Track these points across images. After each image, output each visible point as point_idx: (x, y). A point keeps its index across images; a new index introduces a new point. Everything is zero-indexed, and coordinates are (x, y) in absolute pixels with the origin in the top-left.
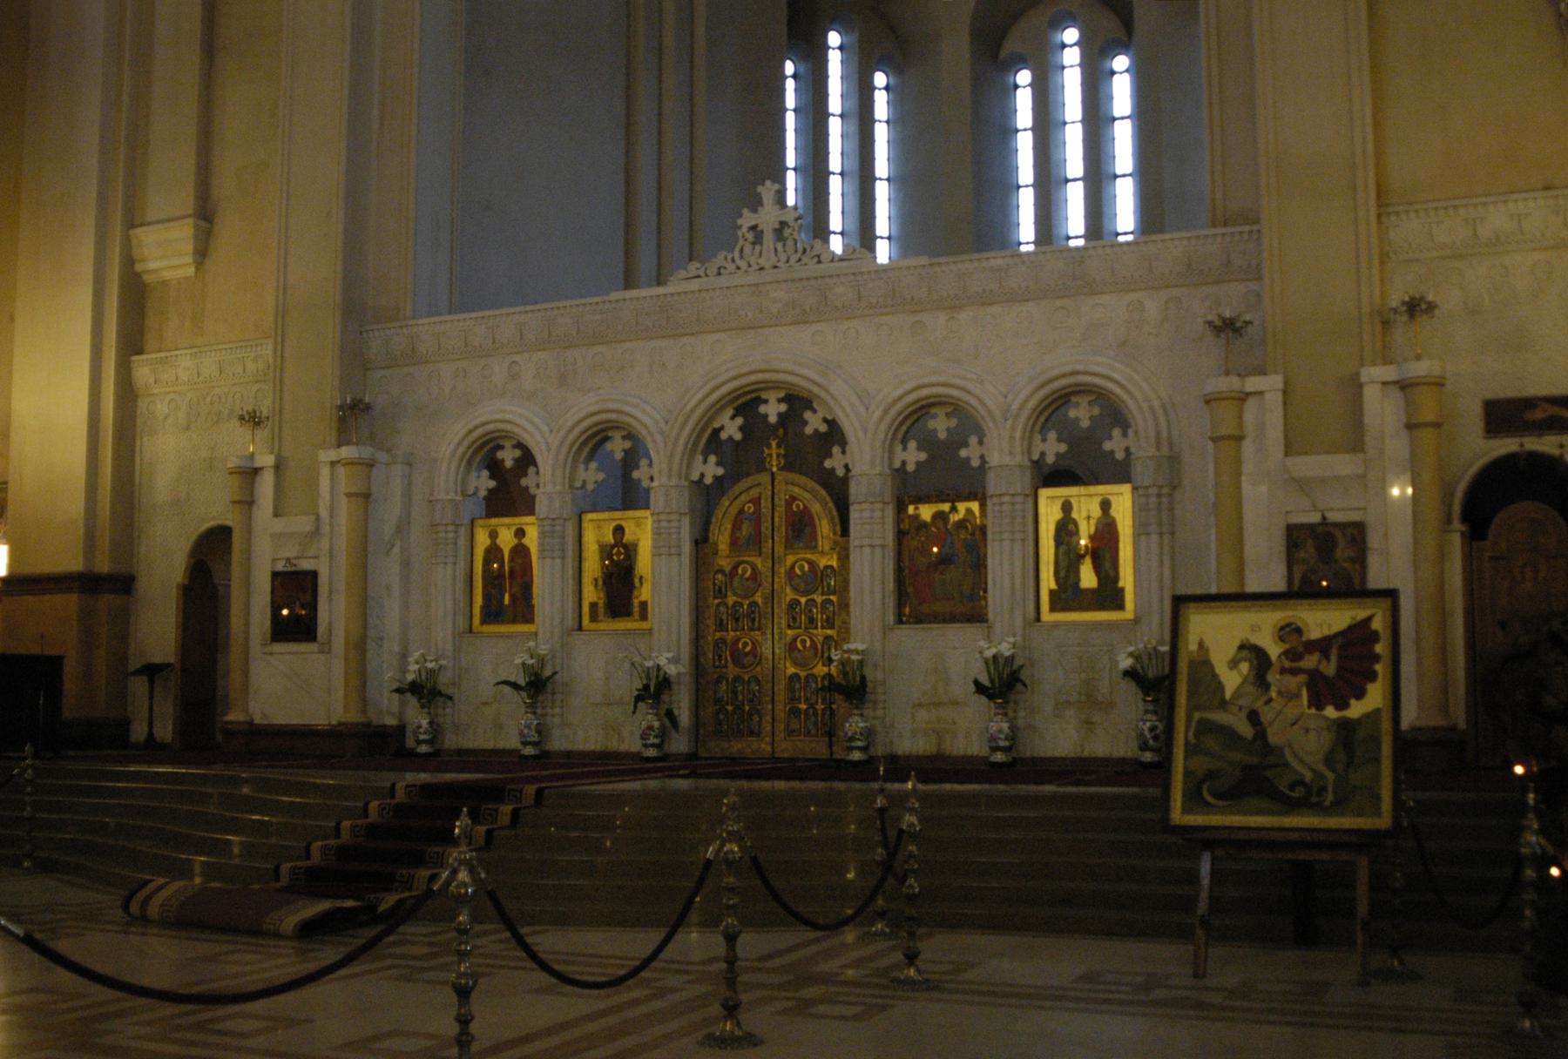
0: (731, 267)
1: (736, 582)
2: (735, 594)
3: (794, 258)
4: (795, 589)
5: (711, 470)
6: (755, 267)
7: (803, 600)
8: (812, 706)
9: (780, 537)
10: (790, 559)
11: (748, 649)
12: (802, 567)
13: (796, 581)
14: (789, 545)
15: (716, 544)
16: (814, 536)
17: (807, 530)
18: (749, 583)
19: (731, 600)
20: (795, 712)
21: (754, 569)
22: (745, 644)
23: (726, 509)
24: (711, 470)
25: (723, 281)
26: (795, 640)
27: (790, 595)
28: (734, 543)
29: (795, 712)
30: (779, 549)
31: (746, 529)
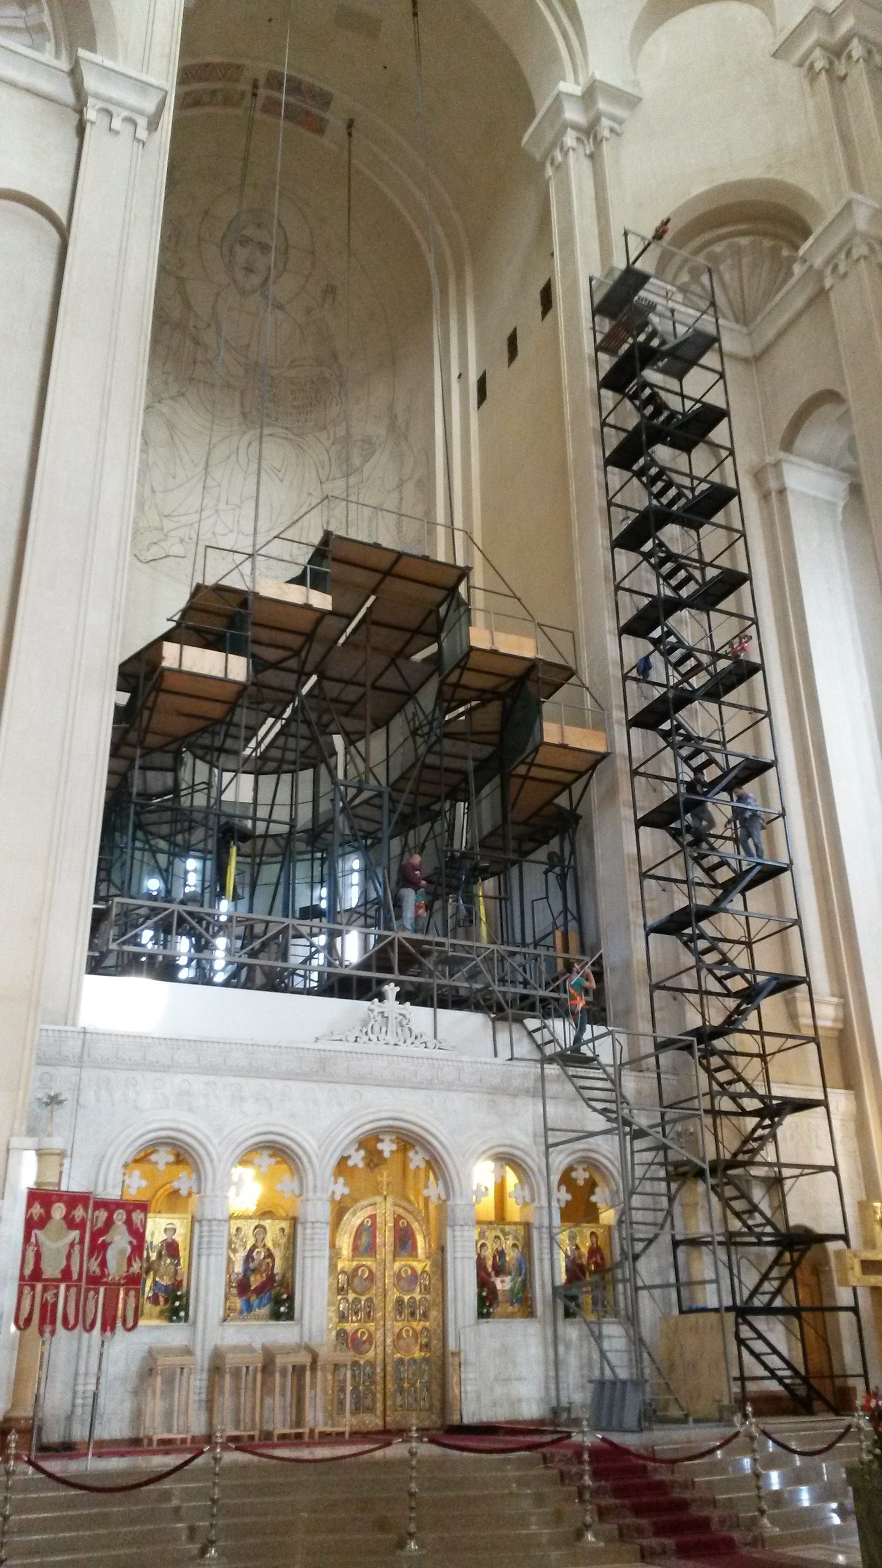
0: (366, 1038)
1: (356, 1281)
2: (354, 1292)
3: (409, 1041)
4: (401, 1289)
5: (341, 1189)
6: (383, 1042)
7: (363, 1298)
8: (413, 1385)
9: (389, 1248)
10: (397, 1265)
11: (365, 1338)
12: (406, 1271)
13: (402, 1283)
14: (396, 1255)
15: (340, 1249)
16: (415, 1247)
17: (410, 1243)
18: (367, 1283)
19: (351, 1296)
20: (401, 1390)
21: (371, 1272)
22: (363, 1333)
23: (354, 1220)
24: (341, 1189)
25: (358, 1047)
26: (401, 1330)
27: (397, 1294)
28: (355, 1248)
29: (401, 1390)
30: (389, 1257)
31: (365, 1239)
